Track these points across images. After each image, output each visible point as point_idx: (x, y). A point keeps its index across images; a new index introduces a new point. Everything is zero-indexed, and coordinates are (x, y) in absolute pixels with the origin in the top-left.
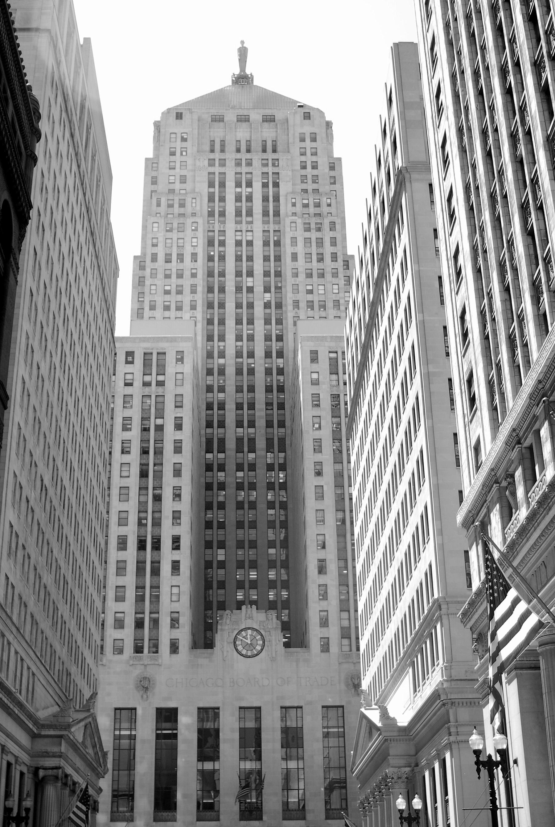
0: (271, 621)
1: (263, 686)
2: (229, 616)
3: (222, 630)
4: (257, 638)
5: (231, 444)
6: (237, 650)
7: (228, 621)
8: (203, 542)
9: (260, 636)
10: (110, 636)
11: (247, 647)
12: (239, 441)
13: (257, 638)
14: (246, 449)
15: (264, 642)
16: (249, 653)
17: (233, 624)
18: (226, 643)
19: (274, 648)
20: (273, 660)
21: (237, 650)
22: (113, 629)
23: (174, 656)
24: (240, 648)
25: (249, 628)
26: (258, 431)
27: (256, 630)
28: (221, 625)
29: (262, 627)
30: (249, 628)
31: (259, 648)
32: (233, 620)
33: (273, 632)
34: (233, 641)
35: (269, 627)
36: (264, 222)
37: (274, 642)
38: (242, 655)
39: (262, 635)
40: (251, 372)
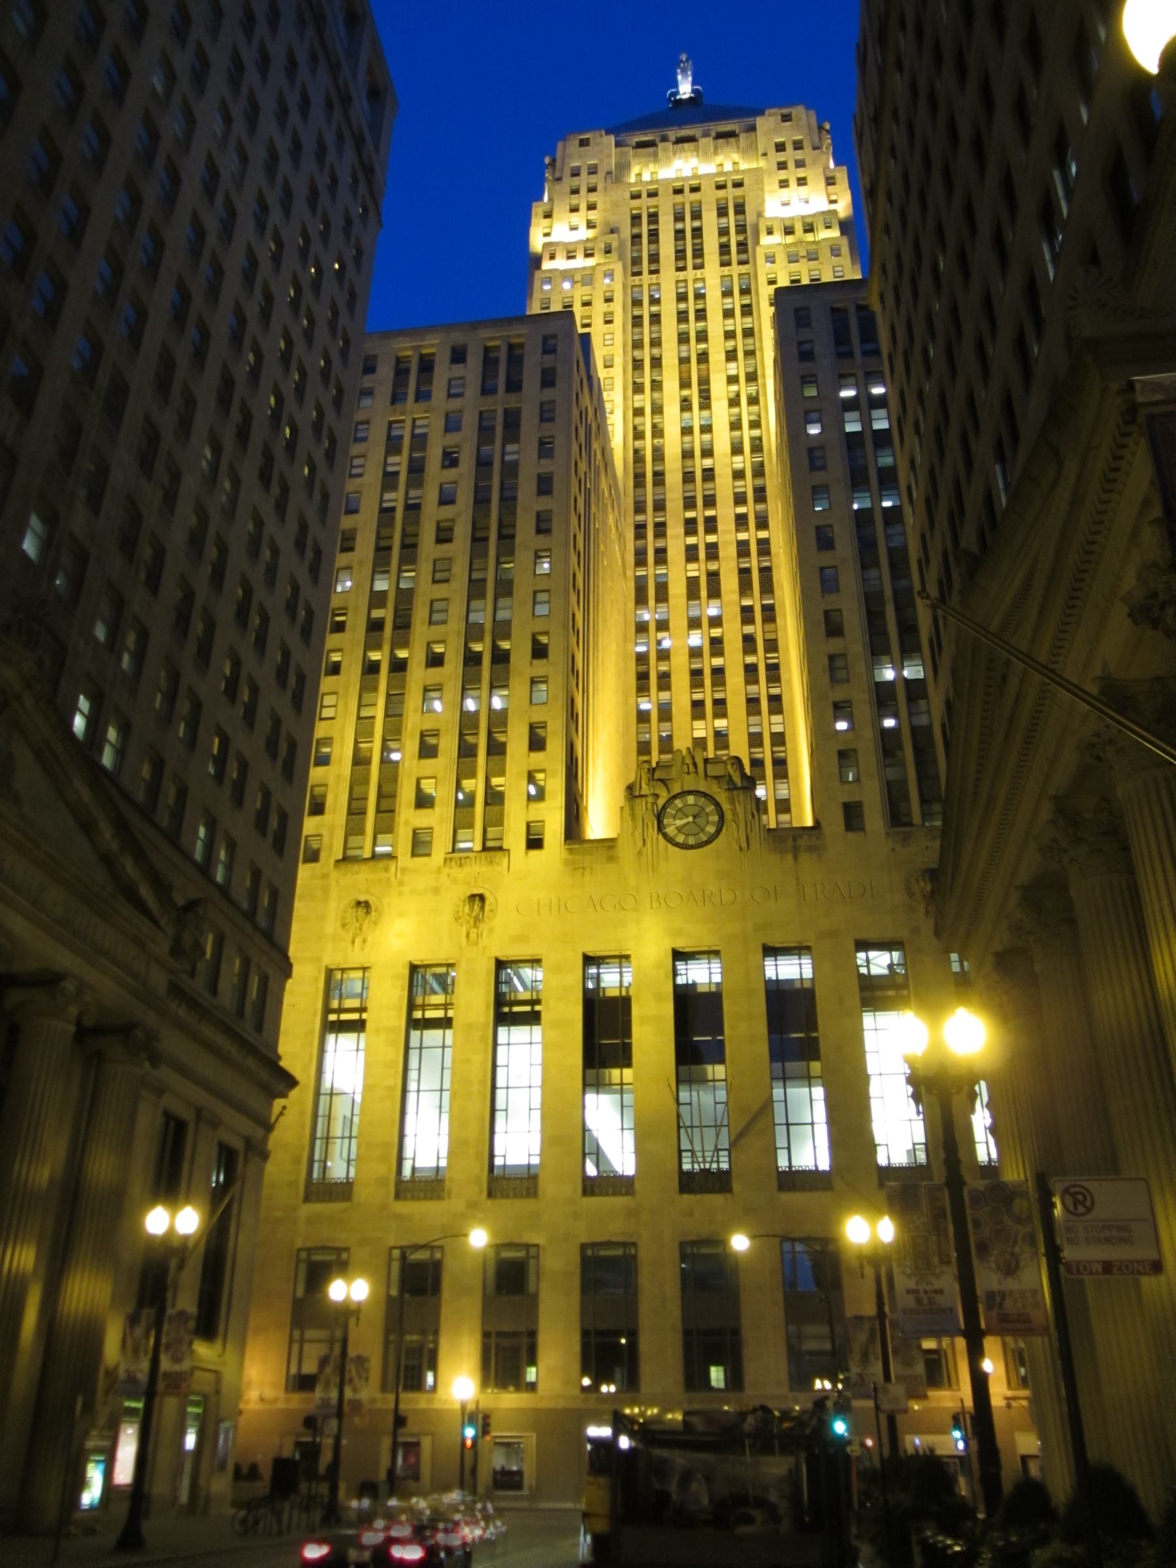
5: (677, 589)
8: (634, 746)
9: (713, 807)
10: (407, 823)
12: (692, 583)
13: (707, 810)
14: (704, 593)
16: (691, 841)
21: (665, 836)
22: (412, 810)
23: (534, 853)
24: (671, 831)
25: (690, 793)
26: (723, 564)
27: (705, 795)
30: (690, 793)
31: (711, 829)
36: (723, 264)
38: (677, 845)
39: (717, 805)
40: (709, 475)
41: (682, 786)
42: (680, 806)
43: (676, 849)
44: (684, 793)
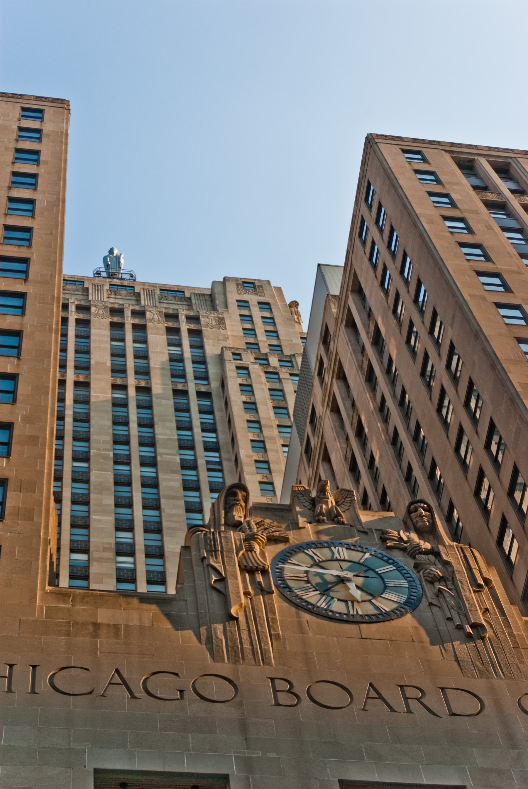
1: (454, 714)
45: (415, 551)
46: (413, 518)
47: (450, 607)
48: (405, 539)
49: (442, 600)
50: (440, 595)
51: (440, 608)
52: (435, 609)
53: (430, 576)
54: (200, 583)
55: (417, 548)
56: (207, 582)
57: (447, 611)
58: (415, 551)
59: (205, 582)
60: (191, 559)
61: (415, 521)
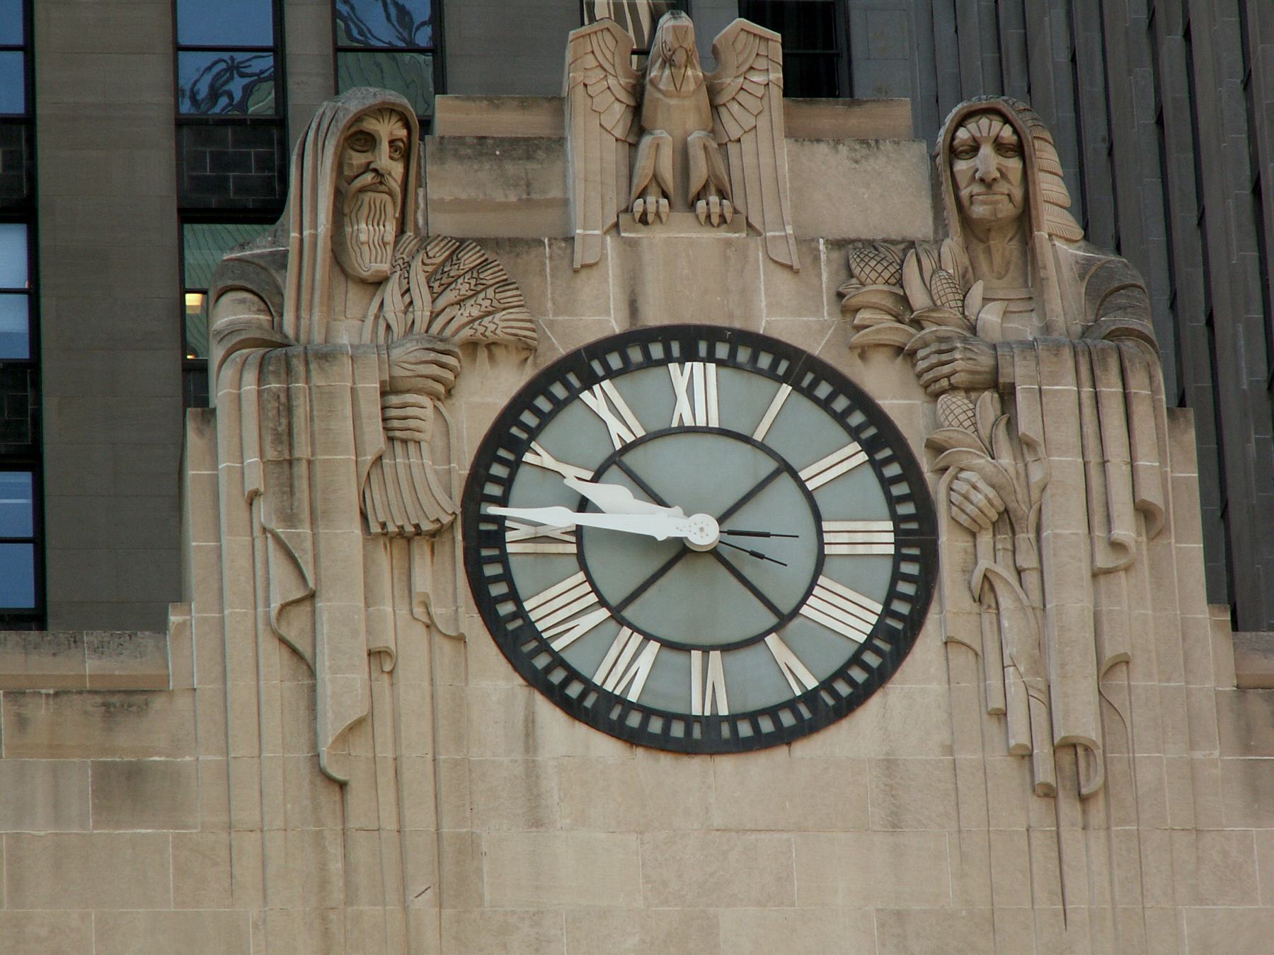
0: (1005, 247)
2: (384, 159)
3: (275, 352)
4: (816, 475)
6: (517, 640)
7: (372, 238)
9: (852, 455)
11: (668, 605)
15: (917, 537)
16: (708, 689)
17: (439, 280)
18: (346, 536)
19: (1072, 600)
20: (1071, 775)
21: (517, 640)
25: (690, 341)
27: (797, 368)
28: (270, 300)
29: (882, 326)
30: (690, 341)
31: (845, 613)
32: (443, 224)
33: (1054, 399)
34: (443, 503)
35: (990, 317)
37: (1065, 524)
39: (880, 437)
41: (633, 308)
42: (619, 433)
43: (604, 747)
44: (644, 347)
45: (936, 380)
46: (962, 181)
47: (1007, 661)
48: (919, 299)
49: (988, 618)
50: (989, 598)
51: (976, 654)
52: (961, 659)
53: (969, 508)
54: (236, 612)
55: (946, 369)
56: (260, 609)
57: (994, 682)
58: (936, 380)
59: (255, 608)
60: (217, 476)
61: (964, 193)
